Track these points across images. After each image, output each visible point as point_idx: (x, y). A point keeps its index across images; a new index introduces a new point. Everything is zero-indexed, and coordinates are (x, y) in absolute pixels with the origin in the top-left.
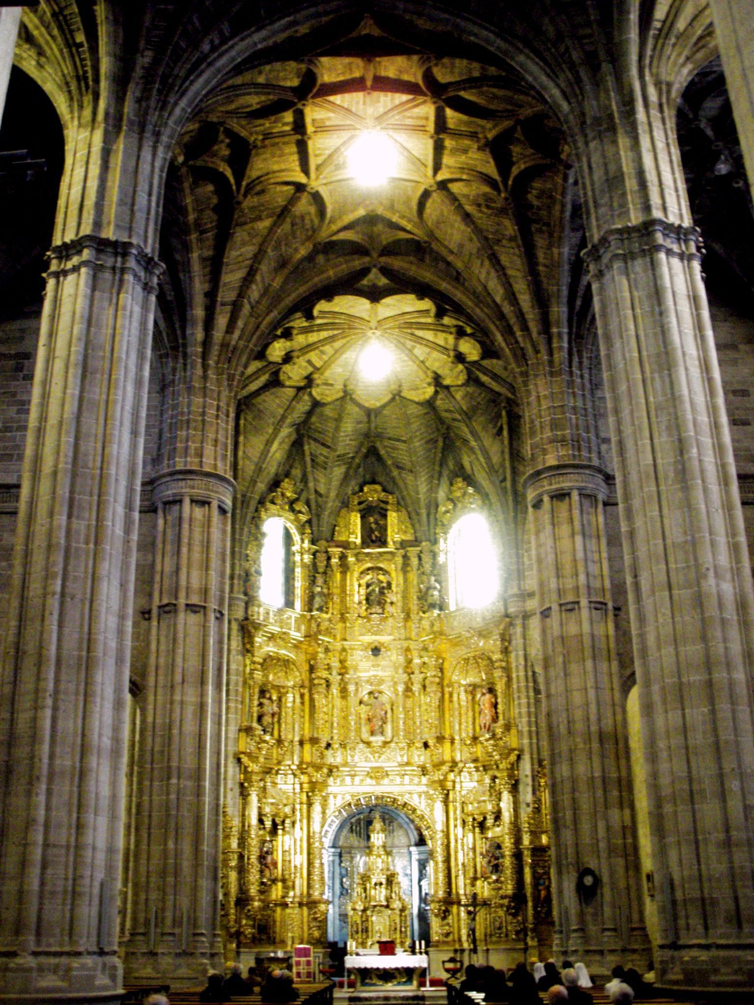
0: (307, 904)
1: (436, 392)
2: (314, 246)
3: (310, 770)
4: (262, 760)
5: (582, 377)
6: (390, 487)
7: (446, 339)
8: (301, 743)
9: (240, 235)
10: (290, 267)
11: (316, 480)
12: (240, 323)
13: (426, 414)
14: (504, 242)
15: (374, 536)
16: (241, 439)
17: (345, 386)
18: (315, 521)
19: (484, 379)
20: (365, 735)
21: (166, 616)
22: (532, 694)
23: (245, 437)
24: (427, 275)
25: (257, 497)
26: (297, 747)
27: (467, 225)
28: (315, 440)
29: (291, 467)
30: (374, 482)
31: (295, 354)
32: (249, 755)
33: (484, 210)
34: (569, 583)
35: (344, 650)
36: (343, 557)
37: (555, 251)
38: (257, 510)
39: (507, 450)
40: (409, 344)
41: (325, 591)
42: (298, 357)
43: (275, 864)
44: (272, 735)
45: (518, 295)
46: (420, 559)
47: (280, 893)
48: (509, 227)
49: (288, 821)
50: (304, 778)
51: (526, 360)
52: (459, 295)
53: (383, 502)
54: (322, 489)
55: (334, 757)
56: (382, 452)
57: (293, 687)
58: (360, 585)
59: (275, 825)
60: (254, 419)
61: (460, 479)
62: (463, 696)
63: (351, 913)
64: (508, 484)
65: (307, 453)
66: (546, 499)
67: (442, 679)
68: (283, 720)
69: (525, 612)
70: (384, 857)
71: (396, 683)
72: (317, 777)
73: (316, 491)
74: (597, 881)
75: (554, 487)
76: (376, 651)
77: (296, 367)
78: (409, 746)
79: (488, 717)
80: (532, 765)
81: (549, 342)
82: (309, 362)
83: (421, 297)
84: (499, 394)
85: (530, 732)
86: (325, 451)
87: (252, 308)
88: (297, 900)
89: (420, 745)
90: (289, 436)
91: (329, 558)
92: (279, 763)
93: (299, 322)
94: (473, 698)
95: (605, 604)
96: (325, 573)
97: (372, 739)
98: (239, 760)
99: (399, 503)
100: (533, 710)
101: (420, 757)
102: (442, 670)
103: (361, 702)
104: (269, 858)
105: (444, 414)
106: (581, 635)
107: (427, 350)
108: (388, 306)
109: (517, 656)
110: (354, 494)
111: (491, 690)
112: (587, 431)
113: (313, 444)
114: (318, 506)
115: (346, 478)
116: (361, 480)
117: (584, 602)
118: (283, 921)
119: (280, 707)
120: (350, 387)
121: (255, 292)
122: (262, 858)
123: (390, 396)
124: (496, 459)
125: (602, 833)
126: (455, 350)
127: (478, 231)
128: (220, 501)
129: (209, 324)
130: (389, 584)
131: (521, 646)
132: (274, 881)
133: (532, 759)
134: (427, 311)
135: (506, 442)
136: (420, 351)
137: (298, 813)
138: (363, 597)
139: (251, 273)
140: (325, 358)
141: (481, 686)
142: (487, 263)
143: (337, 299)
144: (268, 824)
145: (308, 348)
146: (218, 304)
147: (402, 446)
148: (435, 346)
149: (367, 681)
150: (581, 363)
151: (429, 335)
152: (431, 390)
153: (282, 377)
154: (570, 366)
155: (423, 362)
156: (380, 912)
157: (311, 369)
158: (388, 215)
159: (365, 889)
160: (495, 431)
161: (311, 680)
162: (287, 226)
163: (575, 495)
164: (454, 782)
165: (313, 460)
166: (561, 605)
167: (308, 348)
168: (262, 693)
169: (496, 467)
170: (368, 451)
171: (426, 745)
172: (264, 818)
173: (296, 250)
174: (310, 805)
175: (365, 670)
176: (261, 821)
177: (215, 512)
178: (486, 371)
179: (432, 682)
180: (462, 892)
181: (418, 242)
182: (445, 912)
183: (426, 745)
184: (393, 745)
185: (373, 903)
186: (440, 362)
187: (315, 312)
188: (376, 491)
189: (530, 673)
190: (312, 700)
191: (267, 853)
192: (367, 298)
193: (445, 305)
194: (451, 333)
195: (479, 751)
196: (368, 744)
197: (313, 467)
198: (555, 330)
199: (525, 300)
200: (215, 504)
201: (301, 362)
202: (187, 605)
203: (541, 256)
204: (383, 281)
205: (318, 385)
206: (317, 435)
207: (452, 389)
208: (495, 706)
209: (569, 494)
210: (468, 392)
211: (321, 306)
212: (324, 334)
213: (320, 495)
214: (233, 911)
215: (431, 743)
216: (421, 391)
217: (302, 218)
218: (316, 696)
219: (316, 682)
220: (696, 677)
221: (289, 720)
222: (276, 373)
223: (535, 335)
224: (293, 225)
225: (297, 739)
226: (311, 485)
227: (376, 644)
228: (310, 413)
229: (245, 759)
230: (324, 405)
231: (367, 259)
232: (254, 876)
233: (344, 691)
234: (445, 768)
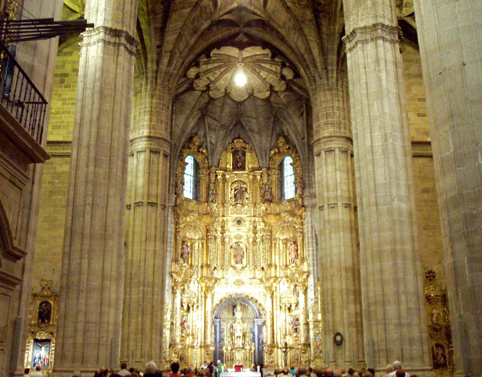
0: (204, 347)
1: (271, 94)
2: (212, 22)
3: (206, 280)
4: (183, 276)
5: (343, 91)
6: (247, 140)
7: (276, 68)
8: (202, 267)
9: (174, 16)
10: (199, 33)
11: (211, 137)
12: (175, 62)
14: (306, 22)
15: (239, 166)
16: (174, 116)
17: (226, 90)
18: (210, 158)
19: (295, 88)
20: (233, 263)
21: (137, 208)
22: (315, 245)
23: (176, 115)
24: (268, 38)
25: (181, 145)
26: (200, 269)
27: (288, 13)
28: (210, 117)
29: (198, 130)
30: (239, 138)
31: (201, 74)
32: (177, 273)
33: (296, 5)
34: (332, 194)
35: (223, 221)
36: (224, 175)
37: (332, 27)
38: (181, 152)
39: (305, 124)
40: (258, 70)
41: (214, 192)
42: (202, 76)
43: (188, 327)
44: (188, 263)
45: (312, 50)
46: (261, 176)
47: (191, 342)
48: (309, 15)
49: (195, 306)
50: (203, 285)
51: (315, 82)
52: (283, 48)
53: (243, 148)
54: (213, 142)
55: (217, 274)
56: (243, 123)
57: (199, 239)
58: (231, 189)
59: (189, 308)
61: (282, 138)
62: (281, 245)
63: (225, 351)
64: (306, 140)
65: (207, 123)
66: (323, 152)
67: (271, 236)
68: (193, 256)
69: (312, 204)
70: (242, 324)
71: (248, 238)
72: (209, 283)
73: (210, 142)
74: (342, 338)
75: (327, 147)
76: (239, 222)
77: (201, 81)
78: (254, 269)
79: (293, 256)
80: (314, 280)
81: (327, 73)
82: (208, 78)
83: (264, 48)
84: (302, 96)
85: (313, 264)
86: (216, 123)
87: (180, 54)
88: (199, 344)
89: (259, 269)
90: (197, 115)
91: (216, 176)
92: (191, 277)
93: (203, 59)
94: (286, 246)
95: (350, 205)
96: (215, 183)
97: (236, 265)
98: (172, 276)
99: (251, 149)
100: (315, 253)
101: (259, 274)
102: (271, 232)
103: (231, 247)
104: (186, 324)
105: (274, 105)
106: (338, 220)
107: (267, 73)
108: (248, 51)
109: (308, 226)
110: (229, 144)
111: (295, 243)
112: (344, 119)
114: (212, 150)
115: (226, 136)
116: (233, 137)
117: (340, 204)
118: (192, 354)
119: (191, 249)
120: (229, 91)
121: (182, 46)
122: (182, 324)
123: (248, 96)
124: (299, 129)
125: (345, 316)
126: (281, 74)
127: (294, 16)
128: (164, 151)
129: (158, 63)
130: (246, 190)
131: (310, 222)
132: (188, 335)
133: (314, 277)
134: (267, 54)
135: (305, 120)
136: (263, 74)
137: (200, 302)
138: (233, 196)
139: (180, 36)
140: (216, 76)
141: (290, 241)
142: (297, 33)
143: (222, 48)
144: (185, 307)
145: (207, 72)
146: (164, 52)
148: (269, 71)
149: (235, 237)
150: (342, 84)
151: (268, 66)
152: (268, 93)
153: (194, 85)
154: (337, 86)
155: (265, 79)
156: (239, 351)
157: (209, 82)
158: (249, 7)
159: (232, 340)
160: (299, 114)
161: (207, 236)
162: (198, 12)
163: (337, 150)
164: (276, 287)
165: (209, 127)
166: (328, 205)
167: (207, 72)
168: (183, 242)
169: (300, 132)
170: (236, 123)
171: (263, 269)
172: (183, 304)
173: (202, 24)
174: (206, 298)
175: (232, 230)
176: (182, 306)
177: (161, 157)
178: (295, 84)
179: (266, 239)
180: (279, 342)
181: (263, 21)
182: (271, 351)
183: (263, 269)
184: (247, 268)
185: (236, 346)
186: (272, 79)
187: (211, 55)
188: (240, 142)
189: (314, 235)
190: (207, 247)
191: (184, 321)
192: (237, 47)
193: (276, 52)
194: (279, 65)
195: (288, 272)
196: (235, 268)
198: (330, 68)
199: (316, 52)
200: (162, 153)
201: (204, 78)
202: (148, 203)
203: (324, 29)
204: (246, 40)
205: (212, 90)
206: (211, 114)
207: (279, 93)
208: (297, 250)
209: (334, 150)
211: (215, 51)
212: (215, 65)
213: (213, 144)
214: (168, 350)
215: (265, 268)
216: (263, 93)
217: (206, 8)
218: (209, 244)
219: (209, 237)
220: (387, 248)
221: (197, 256)
222: (192, 84)
223: (320, 70)
224: (201, 11)
225: (200, 265)
226: (208, 139)
227: (239, 219)
228: (208, 104)
229: (174, 275)
230: (215, 100)
231: (237, 29)
232: (178, 333)
233: (223, 242)
234: (272, 280)
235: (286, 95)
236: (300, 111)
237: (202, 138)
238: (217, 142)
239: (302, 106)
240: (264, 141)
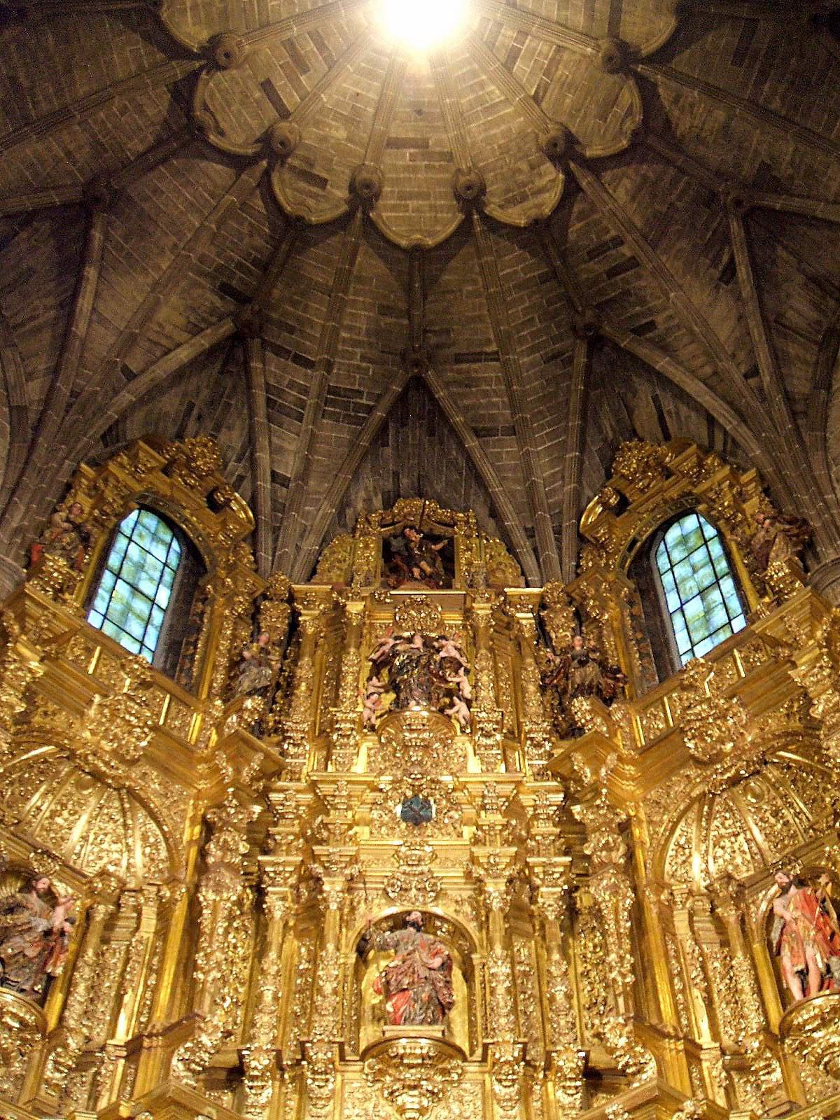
11: (275, 451)
13: (544, 279)
18: (266, 539)
28: (279, 351)
54: (289, 468)
65: (259, 380)
68: (84, 975)
86: (300, 376)
113: (275, 364)
114: (278, 507)
135: (747, 291)
147: (490, 371)
165: (270, 403)
175: (374, 844)
206: (284, 339)
210: (645, 178)
213: (284, 482)
226: (263, 457)
235: (645, 178)
237: (232, 464)
238: (303, 476)
239: (726, 240)
240: (544, 470)
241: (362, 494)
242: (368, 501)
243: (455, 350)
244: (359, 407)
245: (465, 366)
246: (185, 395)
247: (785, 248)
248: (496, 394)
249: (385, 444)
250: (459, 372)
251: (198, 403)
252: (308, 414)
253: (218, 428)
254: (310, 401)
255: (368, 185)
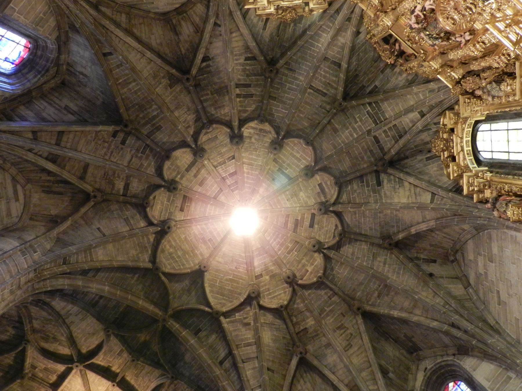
13: (274, 99)
28: (382, 149)
54: (414, 115)
60: (393, 226)
65: (397, 147)
86: (382, 137)
147: (317, 84)
165: (401, 137)
197: (406, 133)
210: (216, 109)
236: (208, 66)
239: (200, 69)
241: (400, 78)
242: (400, 73)
243: (324, 99)
244: (373, 109)
245: (324, 91)
246: (425, 165)
247: (180, 51)
248: (321, 75)
249: (376, 87)
250: (328, 90)
251: (424, 157)
252: (391, 125)
253: (427, 143)
254: (386, 128)
255: (307, 175)
